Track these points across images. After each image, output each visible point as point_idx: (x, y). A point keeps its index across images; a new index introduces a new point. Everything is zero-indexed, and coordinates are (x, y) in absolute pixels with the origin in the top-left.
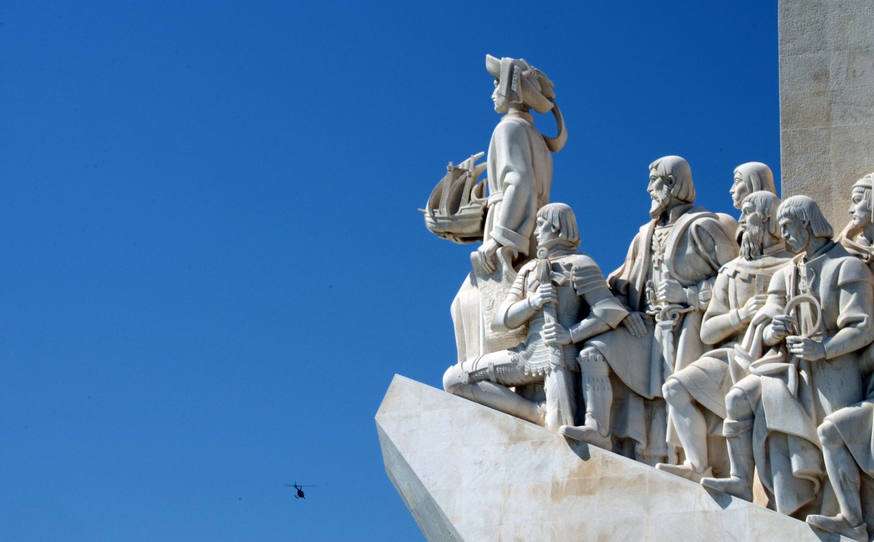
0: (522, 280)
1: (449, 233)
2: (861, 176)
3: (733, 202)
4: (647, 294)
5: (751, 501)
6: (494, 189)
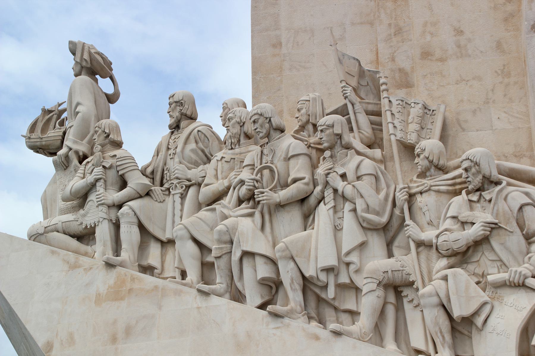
0: (84, 168)
1: (40, 149)
4: (165, 175)
6: (70, 120)
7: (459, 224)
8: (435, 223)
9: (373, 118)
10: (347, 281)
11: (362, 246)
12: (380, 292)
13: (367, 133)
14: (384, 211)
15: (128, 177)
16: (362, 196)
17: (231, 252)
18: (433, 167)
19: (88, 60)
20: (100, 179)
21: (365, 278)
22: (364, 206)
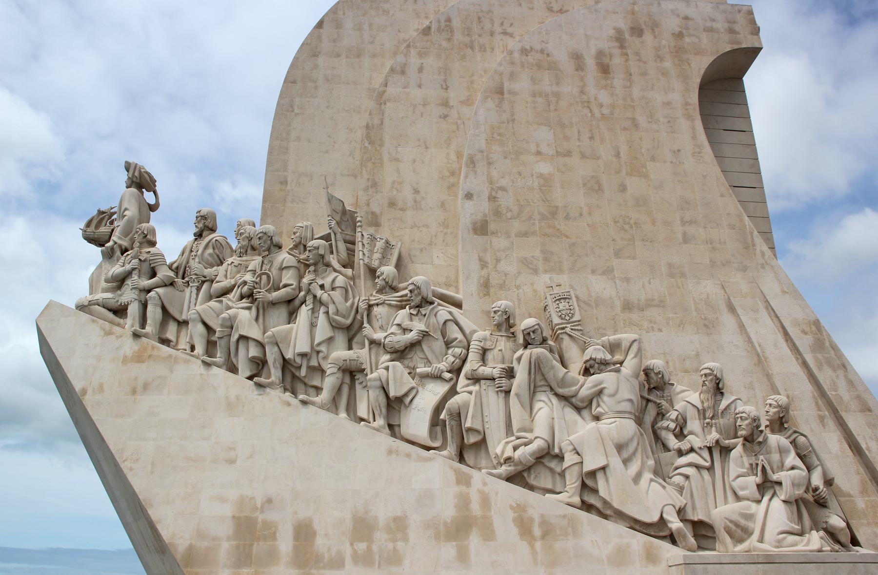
1: (92, 240)
7: (402, 330)
8: (385, 328)
10: (316, 364)
11: (330, 340)
12: (340, 375)
13: (343, 256)
14: (349, 315)
15: (157, 269)
16: (334, 303)
17: (231, 335)
18: (388, 287)
19: (138, 177)
20: (136, 268)
21: (329, 364)
22: (335, 310)
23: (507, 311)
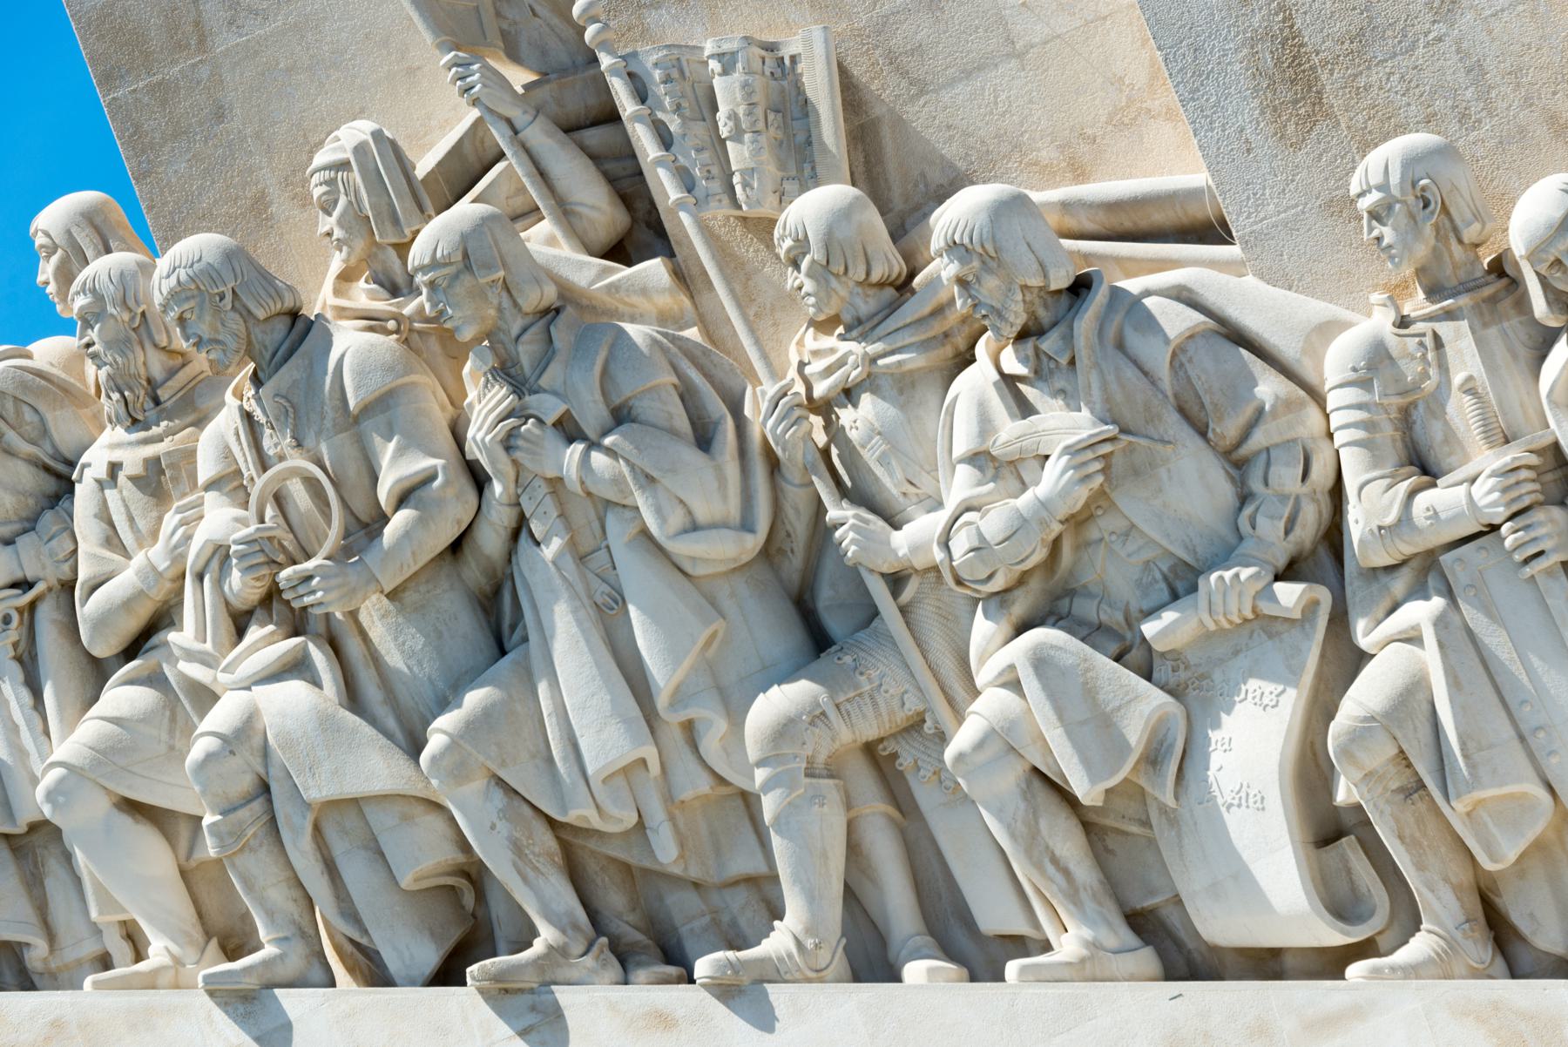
2: (320, 144)
3: (54, 305)
5: (332, 984)
9: (594, 137)
23: (1423, 189)
